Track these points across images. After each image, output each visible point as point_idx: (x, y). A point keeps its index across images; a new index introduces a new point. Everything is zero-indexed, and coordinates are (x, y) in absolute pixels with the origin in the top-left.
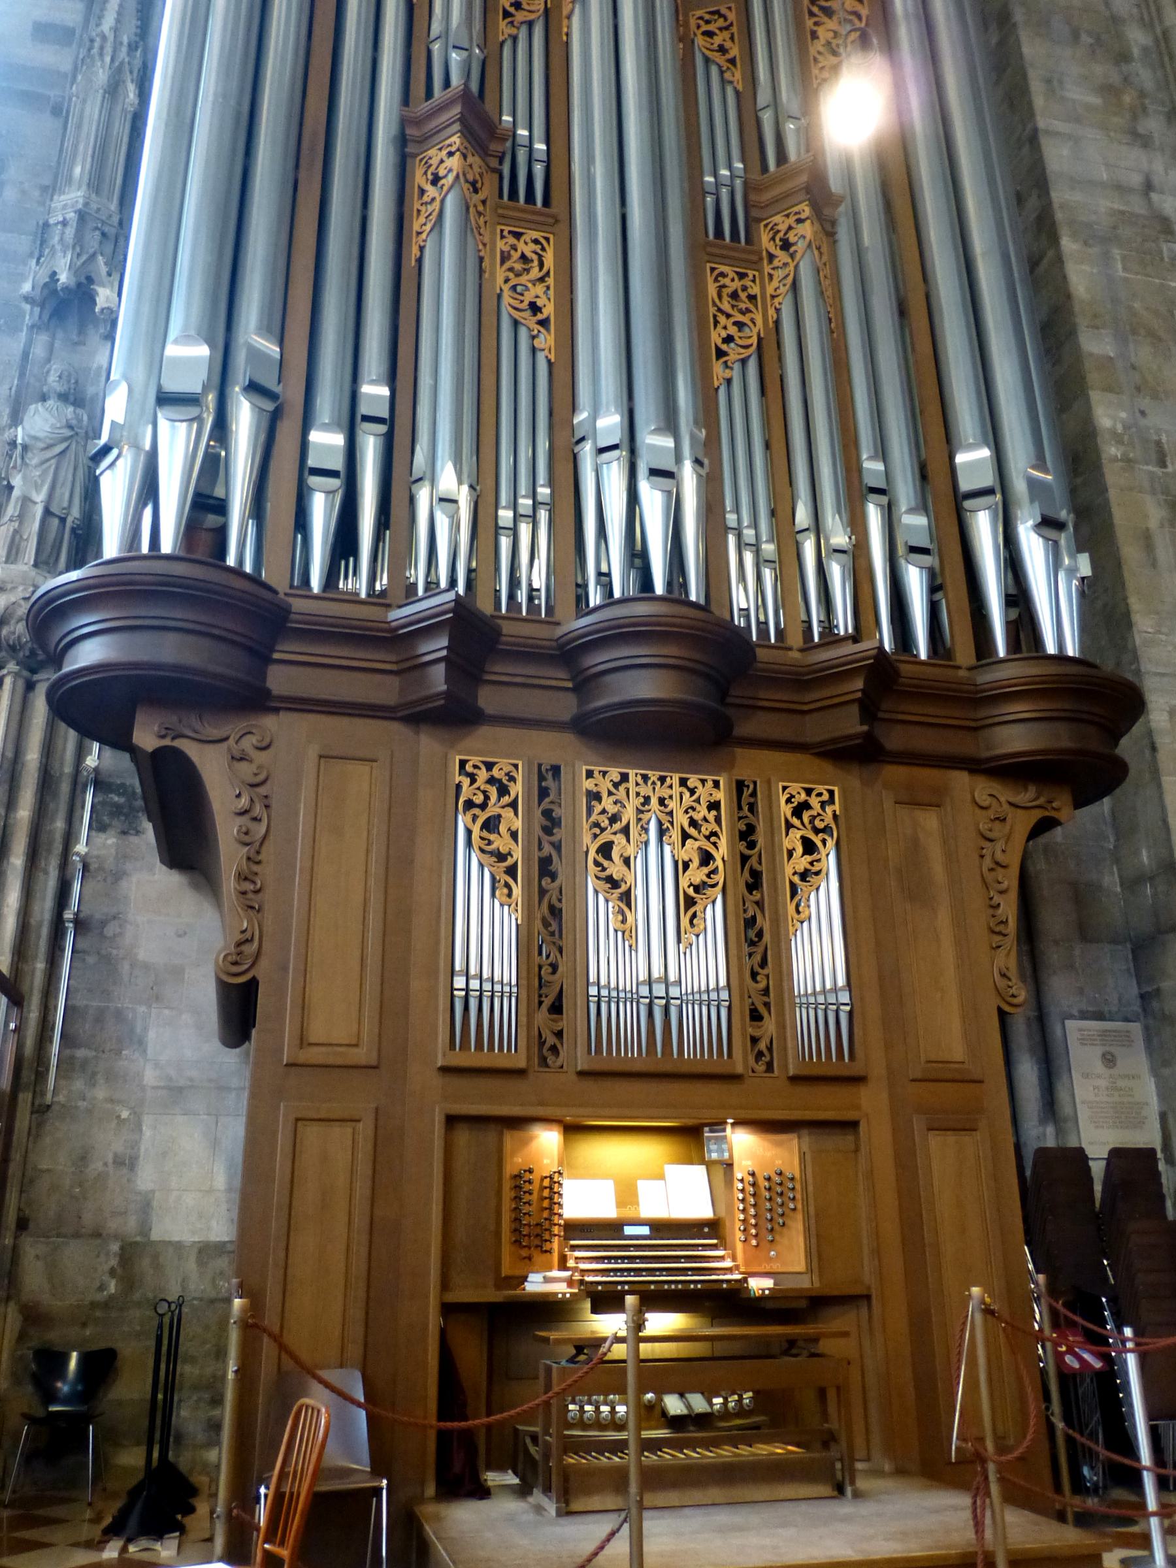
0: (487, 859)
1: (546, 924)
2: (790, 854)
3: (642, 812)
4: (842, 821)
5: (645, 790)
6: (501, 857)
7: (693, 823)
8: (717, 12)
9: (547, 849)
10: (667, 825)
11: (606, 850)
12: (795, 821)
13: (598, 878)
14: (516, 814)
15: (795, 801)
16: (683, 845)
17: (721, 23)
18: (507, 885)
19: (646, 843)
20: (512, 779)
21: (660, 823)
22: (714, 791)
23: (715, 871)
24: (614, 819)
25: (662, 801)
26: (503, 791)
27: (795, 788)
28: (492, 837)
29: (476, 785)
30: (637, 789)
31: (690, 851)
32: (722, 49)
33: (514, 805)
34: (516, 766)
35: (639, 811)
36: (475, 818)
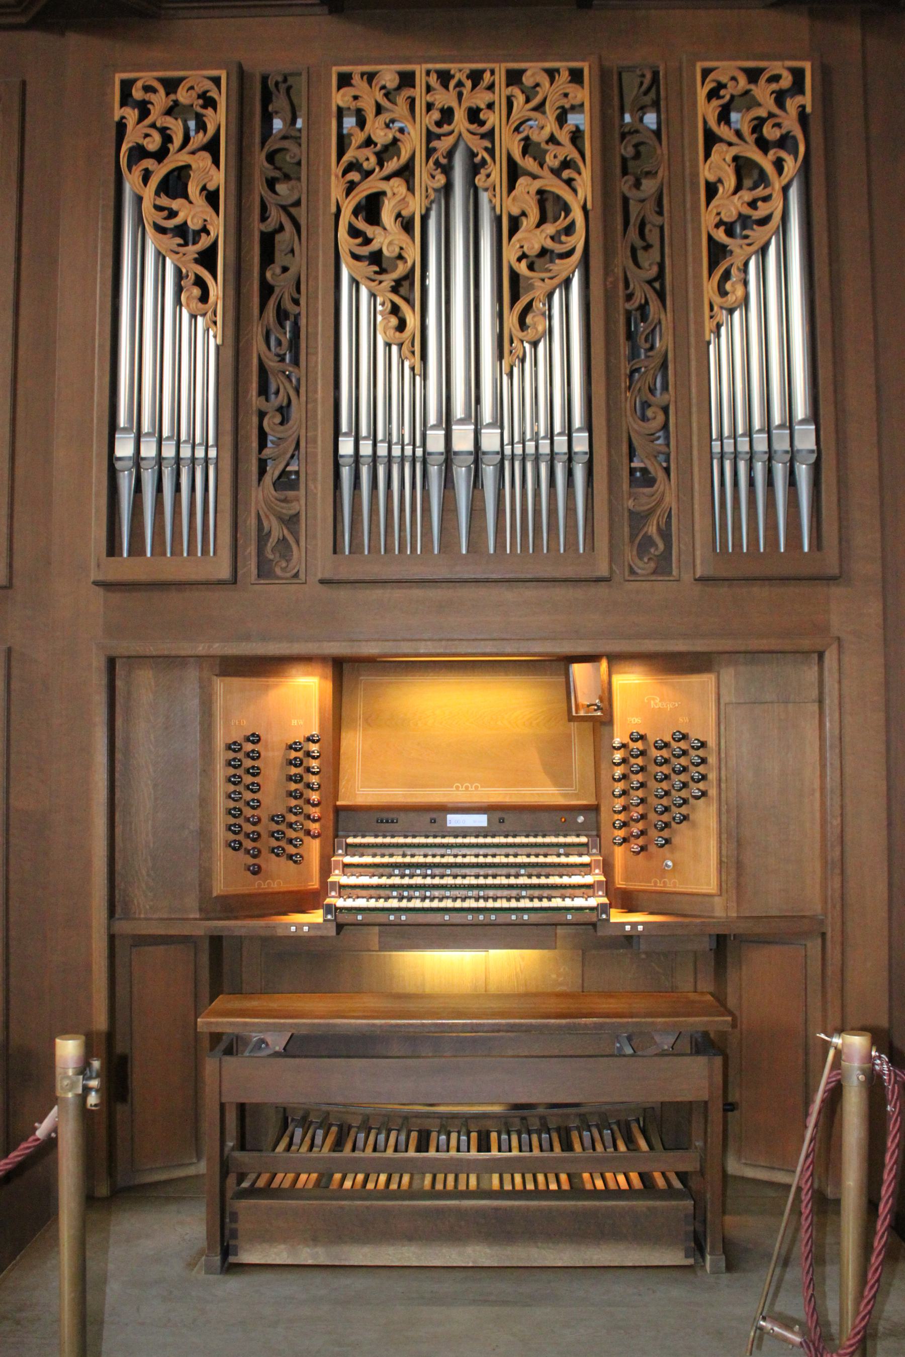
3: (439, 137)
4: (816, 126)
5: (444, 98)
7: (528, 146)
13: (356, 257)
14: (216, 162)
15: (726, 94)
16: (511, 187)
18: (200, 282)
19: (448, 188)
20: (210, 103)
21: (472, 155)
22: (572, 89)
23: (569, 230)
25: (474, 115)
28: (175, 204)
29: (148, 121)
30: (429, 98)
33: (212, 147)
35: (430, 136)
36: (146, 176)
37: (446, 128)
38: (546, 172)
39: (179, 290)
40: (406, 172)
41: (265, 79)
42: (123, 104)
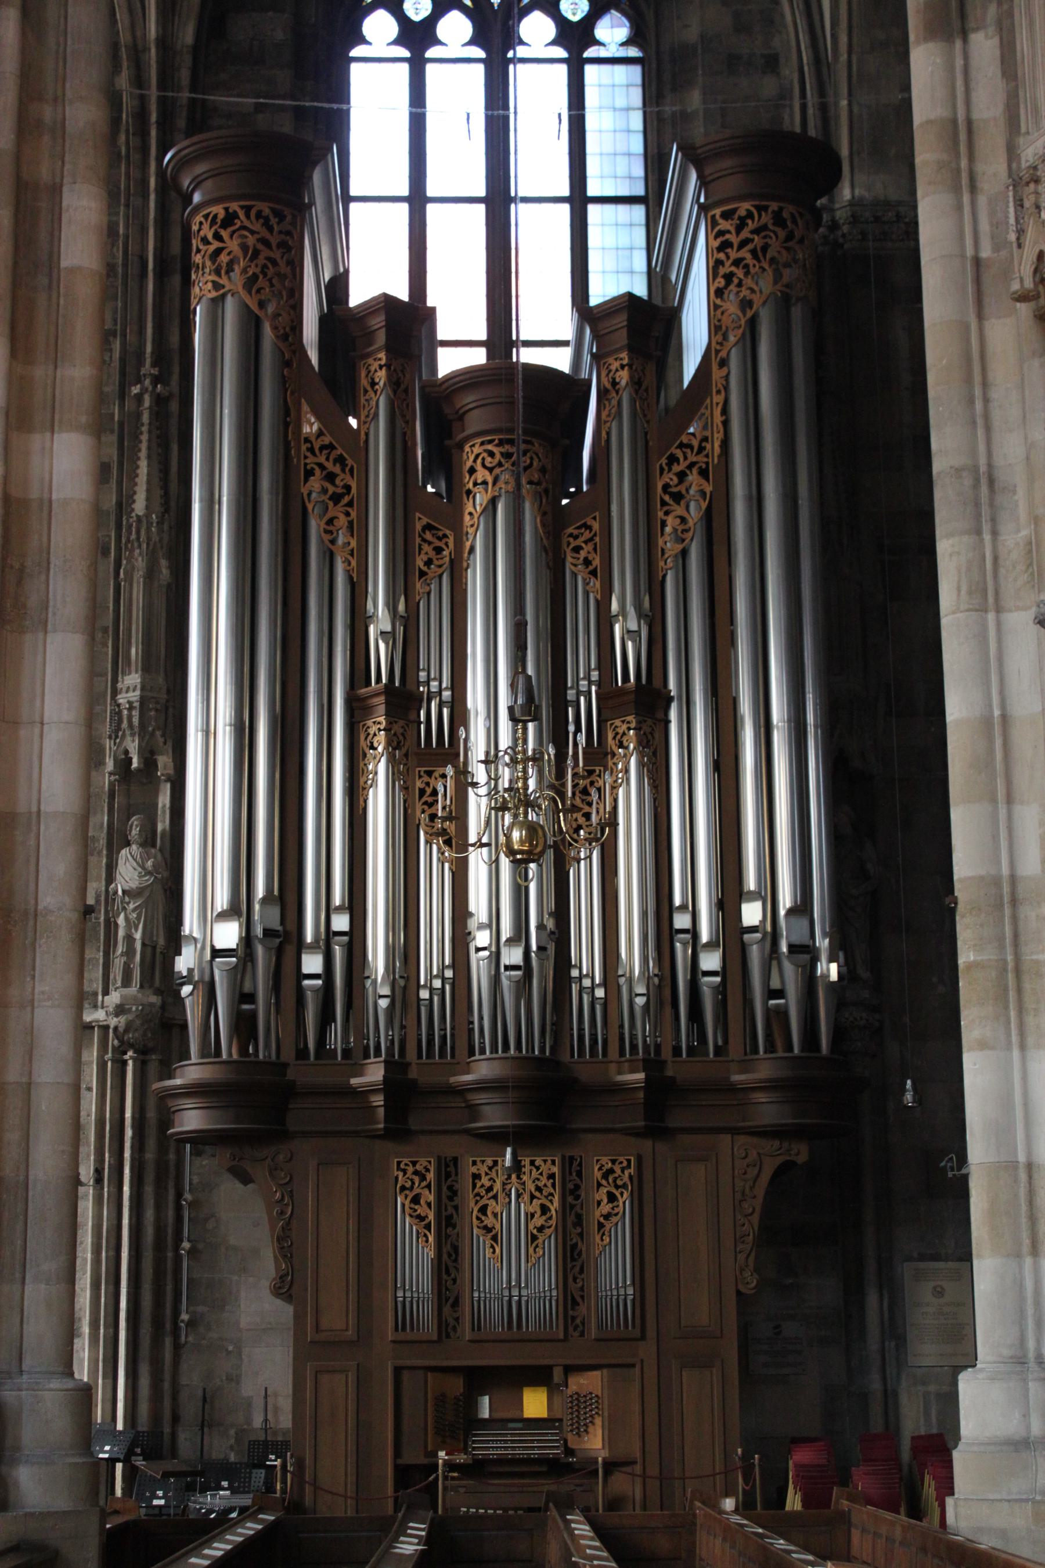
2: (599, 1203)
3: (507, 1184)
6: (421, 1218)
7: (538, 1189)
9: (450, 1210)
10: (521, 1191)
11: (483, 1210)
12: (604, 1182)
13: (478, 1227)
14: (430, 1192)
16: (531, 1203)
17: (587, 535)
18: (425, 1235)
19: (510, 1202)
20: (428, 1170)
21: (517, 1191)
22: (552, 1167)
23: (550, 1218)
24: (490, 1189)
26: (423, 1178)
27: (605, 1160)
28: (416, 1207)
29: (407, 1176)
33: (429, 1186)
34: (430, 1162)
35: (504, 1184)
37: (509, 1181)
38: (543, 1197)
39: (418, 1238)
40: (495, 1197)
41: (446, 1158)
42: (398, 1170)
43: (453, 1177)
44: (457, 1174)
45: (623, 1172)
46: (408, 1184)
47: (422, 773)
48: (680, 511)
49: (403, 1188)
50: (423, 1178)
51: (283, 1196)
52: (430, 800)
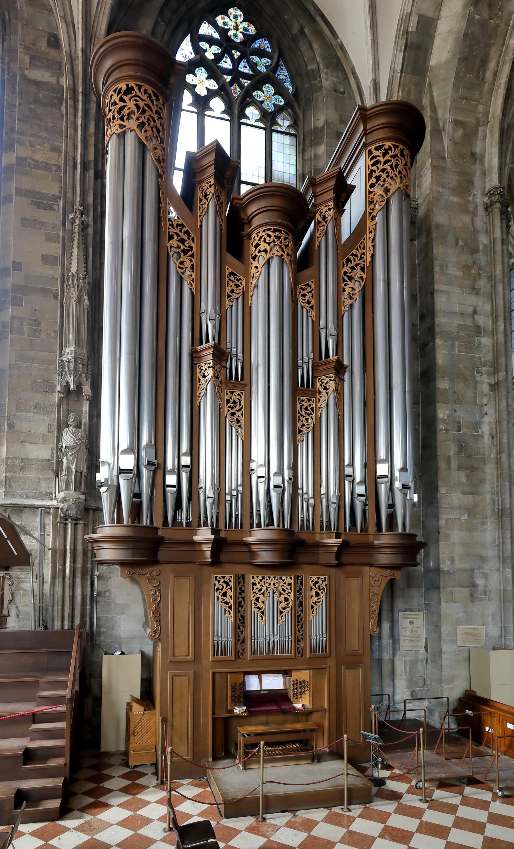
0: (223, 605)
1: (240, 620)
2: (312, 597)
5: (269, 581)
7: (283, 590)
8: (308, 285)
9: (240, 599)
10: (275, 591)
11: (257, 599)
12: (314, 587)
17: (309, 289)
18: (229, 611)
21: (274, 591)
23: (289, 603)
24: (260, 590)
25: (274, 584)
27: (315, 578)
31: (282, 598)
32: (309, 302)
35: (267, 588)
43: (242, 584)
44: (244, 583)
45: (322, 583)
46: (221, 587)
47: (228, 392)
48: (351, 284)
49: (218, 589)
50: (228, 584)
51: (156, 591)
52: (232, 405)
